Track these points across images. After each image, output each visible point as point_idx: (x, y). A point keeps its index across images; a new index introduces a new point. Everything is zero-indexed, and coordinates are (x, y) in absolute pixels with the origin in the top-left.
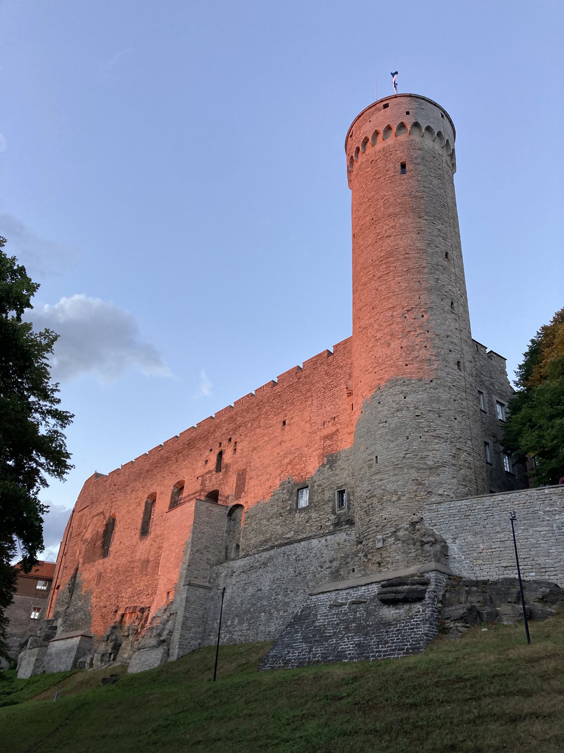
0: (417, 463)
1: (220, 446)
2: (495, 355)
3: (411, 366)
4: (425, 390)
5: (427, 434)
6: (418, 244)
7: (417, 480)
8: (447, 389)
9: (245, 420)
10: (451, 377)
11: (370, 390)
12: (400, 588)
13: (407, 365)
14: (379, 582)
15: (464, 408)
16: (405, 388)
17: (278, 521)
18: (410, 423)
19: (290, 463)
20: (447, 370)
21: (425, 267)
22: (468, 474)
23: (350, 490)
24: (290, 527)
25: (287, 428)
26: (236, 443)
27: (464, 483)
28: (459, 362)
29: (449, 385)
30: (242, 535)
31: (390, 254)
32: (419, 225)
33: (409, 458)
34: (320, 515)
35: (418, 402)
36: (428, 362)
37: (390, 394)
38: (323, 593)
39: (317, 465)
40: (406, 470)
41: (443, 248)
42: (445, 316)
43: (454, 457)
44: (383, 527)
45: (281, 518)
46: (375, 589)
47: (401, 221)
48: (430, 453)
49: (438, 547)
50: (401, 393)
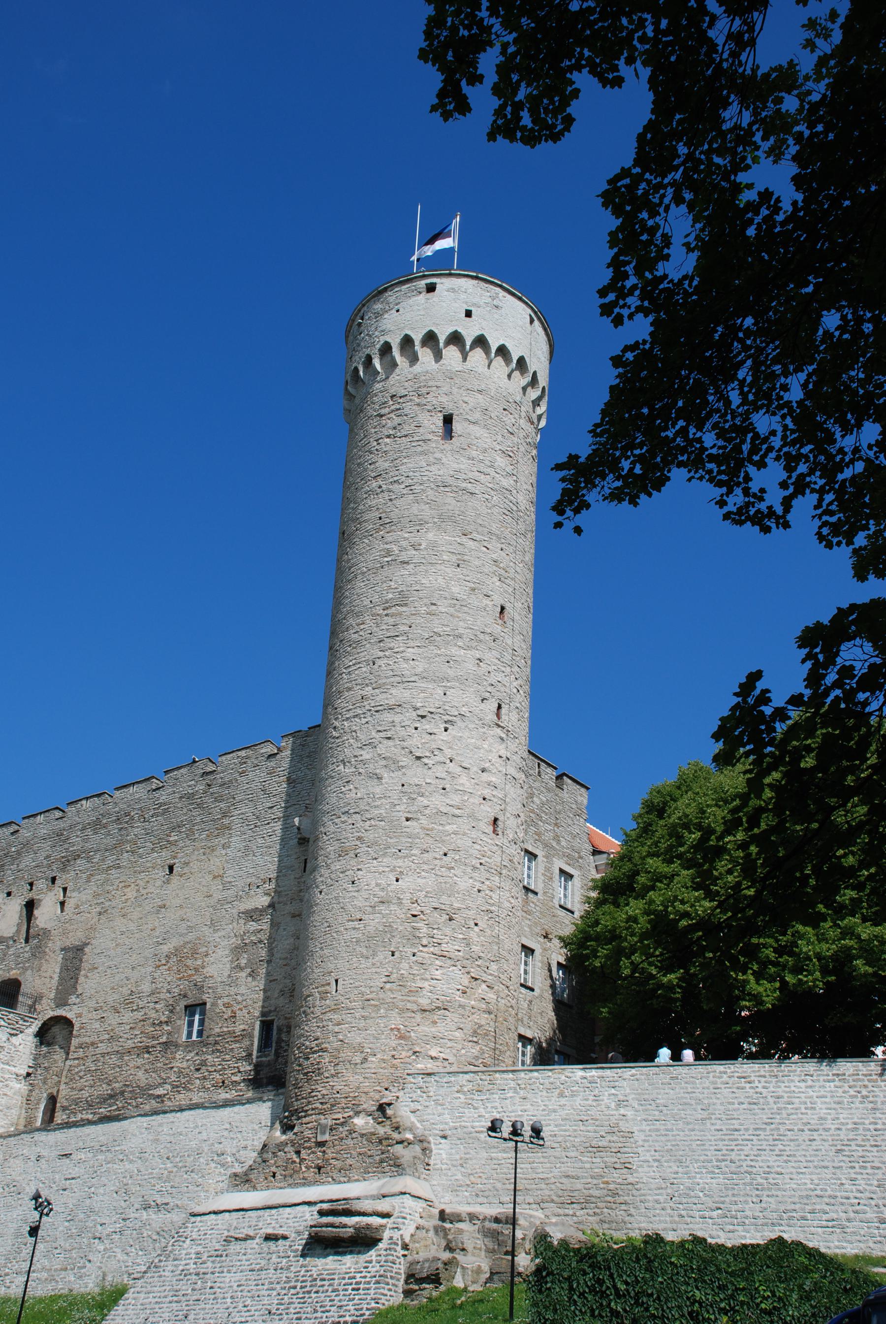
0: (403, 1001)
1: (31, 889)
2: (569, 781)
4: (433, 869)
5: (425, 949)
6: (455, 590)
8: (469, 870)
9: (88, 845)
10: (478, 847)
11: (340, 856)
12: (344, 1220)
14: (315, 1203)
15: (493, 905)
16: (400, 862)
17: (140, 1061)
18: (401, 928)
19: (177, 951)
20: (474, 834)
21: (460, 636)
22: (483, 1022)
23: (282, 1022)
24: (163, 1075)
25: (175, 879)
26: (65, 889)
27: (475, 1039)
28: (496, 820)
29: (474, 862)
30: (63, 1078)
32: (460, 549)
33: (391, 990)
34: (223, 1060)
35: (419, 891)
36: (444, 818)
37: (373, 869)
38: (215, 1213)
40: (382, 1011)
41: (499, 601)
42: (484, 733)
43: (464, 992)
44: (332, 1105)
45: (146, 1056)
46: (309, 1216)
47: (430, 536)
48: (426, 984)
49: (417, 1148)
50: (391, 871)
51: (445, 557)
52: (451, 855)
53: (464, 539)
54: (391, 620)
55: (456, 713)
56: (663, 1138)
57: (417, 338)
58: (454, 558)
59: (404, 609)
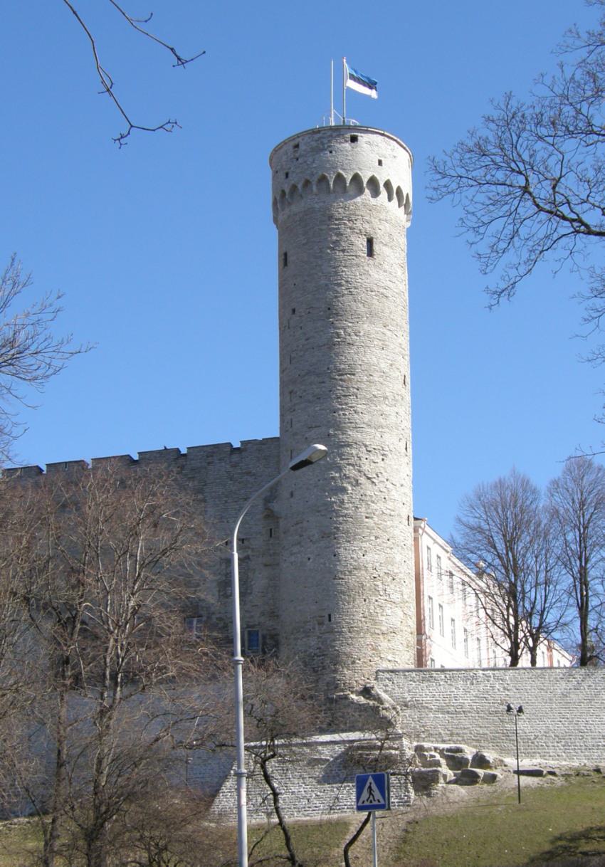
3: (370, 520)
5: (382, 598)
7: (372, 645)
11: (323, 537)
13: (367, 517)
16: (364, 545)
23: (265, 632)
39: (217, 593)
46: (339, 749)
51: (375, 343)
52: (391, 540)
53: (385, 330)
54: (344, 384)
55: (388, 449)
56: (531, 707)
58: (380, 343)
59: (353, 377)
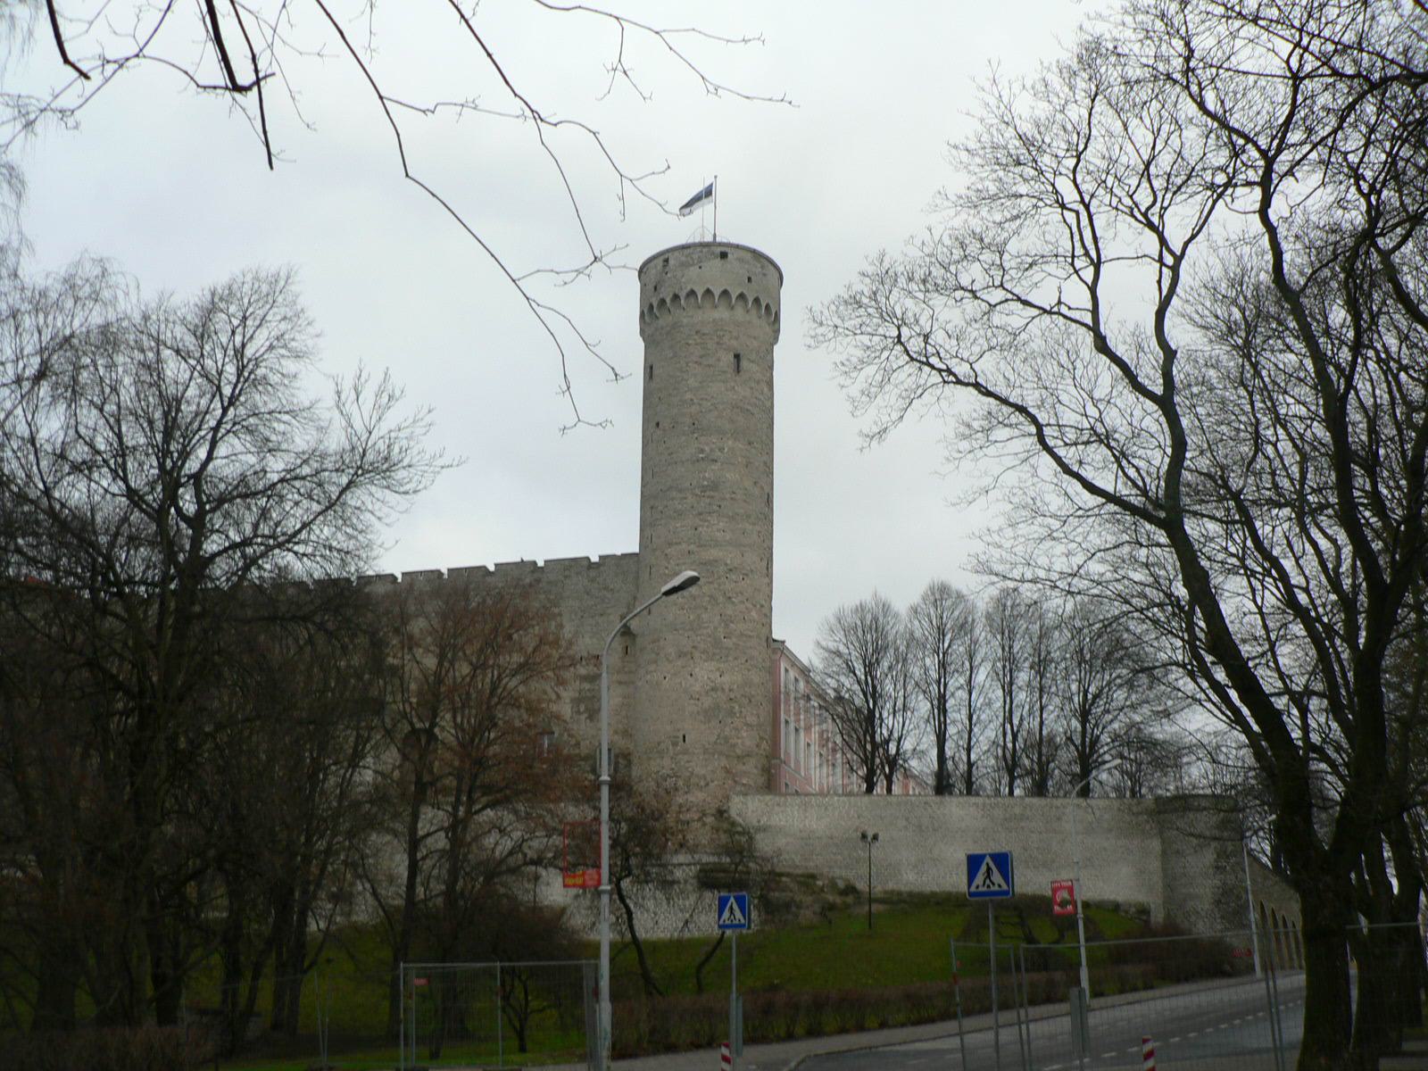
31: (714, 486)
57: (717, 293)
